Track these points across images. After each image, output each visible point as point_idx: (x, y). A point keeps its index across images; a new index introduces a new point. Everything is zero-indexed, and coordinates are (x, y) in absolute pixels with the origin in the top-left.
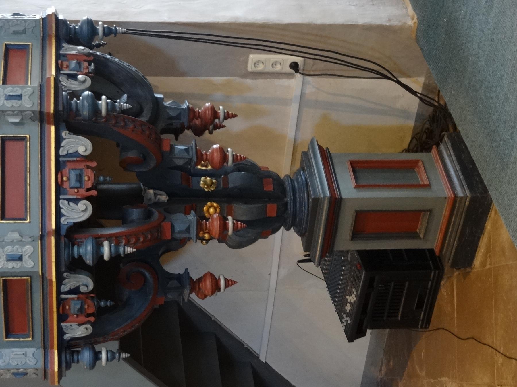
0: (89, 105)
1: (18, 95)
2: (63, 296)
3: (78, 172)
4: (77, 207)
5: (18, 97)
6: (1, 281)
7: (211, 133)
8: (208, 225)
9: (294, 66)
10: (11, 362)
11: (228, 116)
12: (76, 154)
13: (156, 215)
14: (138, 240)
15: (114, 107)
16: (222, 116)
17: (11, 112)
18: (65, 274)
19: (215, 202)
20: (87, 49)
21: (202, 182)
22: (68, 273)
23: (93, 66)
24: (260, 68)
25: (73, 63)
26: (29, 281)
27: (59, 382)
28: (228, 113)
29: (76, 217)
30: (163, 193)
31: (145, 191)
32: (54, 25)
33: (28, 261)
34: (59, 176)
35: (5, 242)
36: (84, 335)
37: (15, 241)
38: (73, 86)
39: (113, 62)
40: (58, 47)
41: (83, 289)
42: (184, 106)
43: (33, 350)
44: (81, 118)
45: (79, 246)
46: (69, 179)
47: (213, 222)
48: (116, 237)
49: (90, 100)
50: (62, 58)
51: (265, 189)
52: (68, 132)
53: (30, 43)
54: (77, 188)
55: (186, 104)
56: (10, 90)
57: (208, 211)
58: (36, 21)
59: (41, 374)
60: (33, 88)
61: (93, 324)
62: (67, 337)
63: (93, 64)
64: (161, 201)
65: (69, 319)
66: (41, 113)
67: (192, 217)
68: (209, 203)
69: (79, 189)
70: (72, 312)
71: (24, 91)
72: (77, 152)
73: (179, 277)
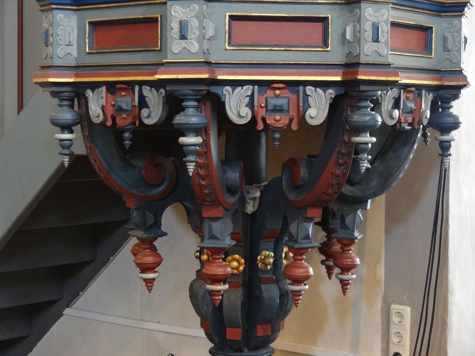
0: (365, 122)
1: (378, 38)
2: (137, 89)
3: (285, 108)
4: (244, 105)
5: (375, 38)
6: (156, 16)
7: (323, 262)
8: (218, 261)
10: (61, 27)
11: (344, 284)
12: (307, 106)
13: (231, 200)
14: (203, 177)
15: (364, 151)
16: (345, 277)
17: (358, 29)
18: (163, 91)
19: (244, 267)
20: (427, 121)
21: (268, 253)
22: (164, 95)
23: (408, 128)
24: (395, 319)
25: (411, 105)
26: (155, 49)
27: (36, 83)
28: (349, 284)
29: (232, 105)
30: (256, 208)
31: (259, 187)
32: (454, 83)
33: (180, 47)
34: (281, 85)
35: (203, 20)
36: (91, 113)
37: (204, 31)
38: (386, 103)
39: (409, 152)
40: (429, 88)
41: (145, 112)
42: (356, 234)
43: (75, 54)
44: (349, 113)
45: (197, 108)
46: (277, 96)
47: (222, 266)
48: (206, 152)
49: (371, 123)
50: (417, 92)
51: (258, 326)
52: (333, 97)
53: (433, 56)
54: (266, 106)
55: (359, 236)
56: (385, 28)
57: (234, 260)
58: (459, 62)
59: (46, 63)
60: (386, 56)
61: (103, 124)
62: (89, 93)
63: (410, 128)
64: (247, 205)
65: (110, 96)
66: (358, 64)
67: (228, 242)
68: (243, 261)
69: (265, 108)
70: (117, 99)
71: (382, 44)
72: (310, 107)
73: (157, 224)
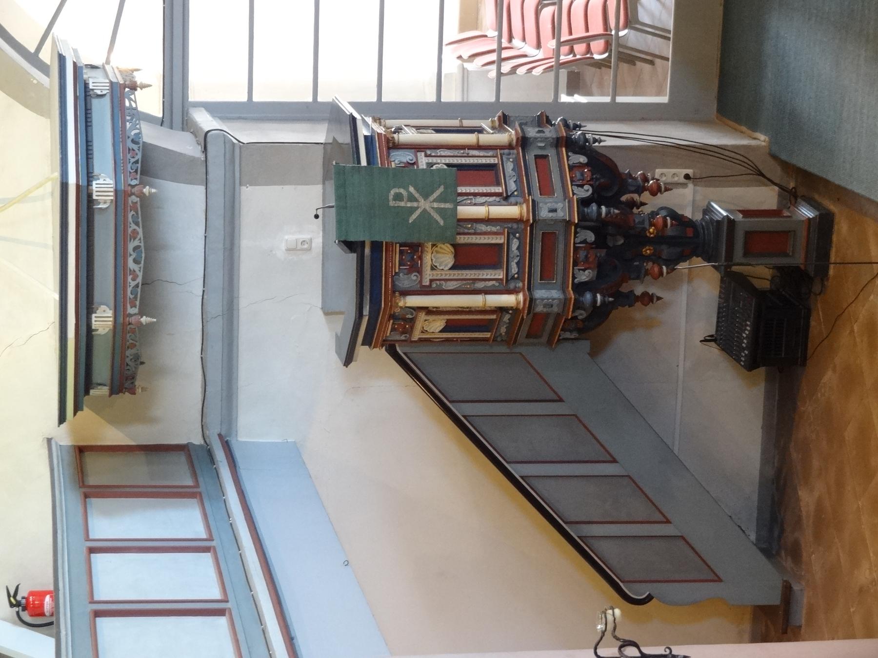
9: (687, 177)
12: (580, 163)
46: (576, 176)
70: (581, 259)
